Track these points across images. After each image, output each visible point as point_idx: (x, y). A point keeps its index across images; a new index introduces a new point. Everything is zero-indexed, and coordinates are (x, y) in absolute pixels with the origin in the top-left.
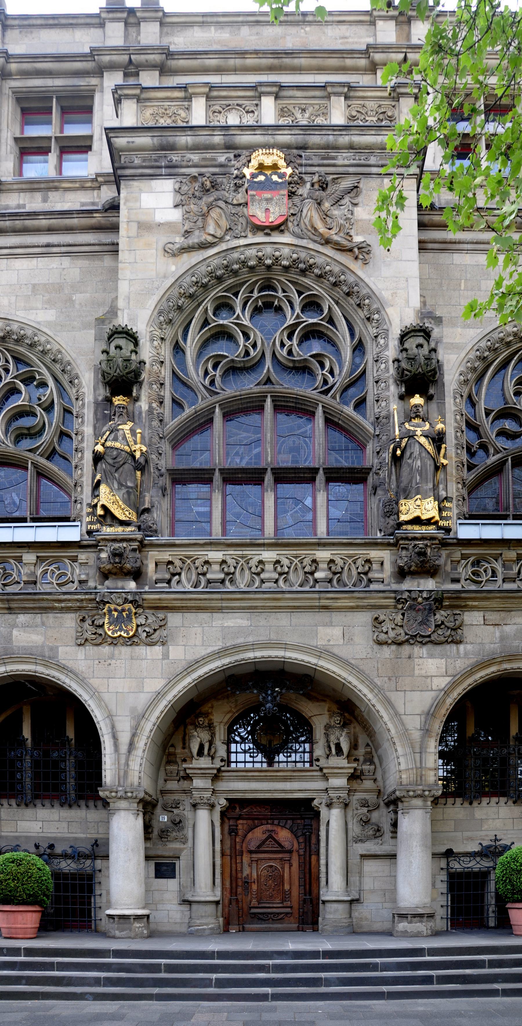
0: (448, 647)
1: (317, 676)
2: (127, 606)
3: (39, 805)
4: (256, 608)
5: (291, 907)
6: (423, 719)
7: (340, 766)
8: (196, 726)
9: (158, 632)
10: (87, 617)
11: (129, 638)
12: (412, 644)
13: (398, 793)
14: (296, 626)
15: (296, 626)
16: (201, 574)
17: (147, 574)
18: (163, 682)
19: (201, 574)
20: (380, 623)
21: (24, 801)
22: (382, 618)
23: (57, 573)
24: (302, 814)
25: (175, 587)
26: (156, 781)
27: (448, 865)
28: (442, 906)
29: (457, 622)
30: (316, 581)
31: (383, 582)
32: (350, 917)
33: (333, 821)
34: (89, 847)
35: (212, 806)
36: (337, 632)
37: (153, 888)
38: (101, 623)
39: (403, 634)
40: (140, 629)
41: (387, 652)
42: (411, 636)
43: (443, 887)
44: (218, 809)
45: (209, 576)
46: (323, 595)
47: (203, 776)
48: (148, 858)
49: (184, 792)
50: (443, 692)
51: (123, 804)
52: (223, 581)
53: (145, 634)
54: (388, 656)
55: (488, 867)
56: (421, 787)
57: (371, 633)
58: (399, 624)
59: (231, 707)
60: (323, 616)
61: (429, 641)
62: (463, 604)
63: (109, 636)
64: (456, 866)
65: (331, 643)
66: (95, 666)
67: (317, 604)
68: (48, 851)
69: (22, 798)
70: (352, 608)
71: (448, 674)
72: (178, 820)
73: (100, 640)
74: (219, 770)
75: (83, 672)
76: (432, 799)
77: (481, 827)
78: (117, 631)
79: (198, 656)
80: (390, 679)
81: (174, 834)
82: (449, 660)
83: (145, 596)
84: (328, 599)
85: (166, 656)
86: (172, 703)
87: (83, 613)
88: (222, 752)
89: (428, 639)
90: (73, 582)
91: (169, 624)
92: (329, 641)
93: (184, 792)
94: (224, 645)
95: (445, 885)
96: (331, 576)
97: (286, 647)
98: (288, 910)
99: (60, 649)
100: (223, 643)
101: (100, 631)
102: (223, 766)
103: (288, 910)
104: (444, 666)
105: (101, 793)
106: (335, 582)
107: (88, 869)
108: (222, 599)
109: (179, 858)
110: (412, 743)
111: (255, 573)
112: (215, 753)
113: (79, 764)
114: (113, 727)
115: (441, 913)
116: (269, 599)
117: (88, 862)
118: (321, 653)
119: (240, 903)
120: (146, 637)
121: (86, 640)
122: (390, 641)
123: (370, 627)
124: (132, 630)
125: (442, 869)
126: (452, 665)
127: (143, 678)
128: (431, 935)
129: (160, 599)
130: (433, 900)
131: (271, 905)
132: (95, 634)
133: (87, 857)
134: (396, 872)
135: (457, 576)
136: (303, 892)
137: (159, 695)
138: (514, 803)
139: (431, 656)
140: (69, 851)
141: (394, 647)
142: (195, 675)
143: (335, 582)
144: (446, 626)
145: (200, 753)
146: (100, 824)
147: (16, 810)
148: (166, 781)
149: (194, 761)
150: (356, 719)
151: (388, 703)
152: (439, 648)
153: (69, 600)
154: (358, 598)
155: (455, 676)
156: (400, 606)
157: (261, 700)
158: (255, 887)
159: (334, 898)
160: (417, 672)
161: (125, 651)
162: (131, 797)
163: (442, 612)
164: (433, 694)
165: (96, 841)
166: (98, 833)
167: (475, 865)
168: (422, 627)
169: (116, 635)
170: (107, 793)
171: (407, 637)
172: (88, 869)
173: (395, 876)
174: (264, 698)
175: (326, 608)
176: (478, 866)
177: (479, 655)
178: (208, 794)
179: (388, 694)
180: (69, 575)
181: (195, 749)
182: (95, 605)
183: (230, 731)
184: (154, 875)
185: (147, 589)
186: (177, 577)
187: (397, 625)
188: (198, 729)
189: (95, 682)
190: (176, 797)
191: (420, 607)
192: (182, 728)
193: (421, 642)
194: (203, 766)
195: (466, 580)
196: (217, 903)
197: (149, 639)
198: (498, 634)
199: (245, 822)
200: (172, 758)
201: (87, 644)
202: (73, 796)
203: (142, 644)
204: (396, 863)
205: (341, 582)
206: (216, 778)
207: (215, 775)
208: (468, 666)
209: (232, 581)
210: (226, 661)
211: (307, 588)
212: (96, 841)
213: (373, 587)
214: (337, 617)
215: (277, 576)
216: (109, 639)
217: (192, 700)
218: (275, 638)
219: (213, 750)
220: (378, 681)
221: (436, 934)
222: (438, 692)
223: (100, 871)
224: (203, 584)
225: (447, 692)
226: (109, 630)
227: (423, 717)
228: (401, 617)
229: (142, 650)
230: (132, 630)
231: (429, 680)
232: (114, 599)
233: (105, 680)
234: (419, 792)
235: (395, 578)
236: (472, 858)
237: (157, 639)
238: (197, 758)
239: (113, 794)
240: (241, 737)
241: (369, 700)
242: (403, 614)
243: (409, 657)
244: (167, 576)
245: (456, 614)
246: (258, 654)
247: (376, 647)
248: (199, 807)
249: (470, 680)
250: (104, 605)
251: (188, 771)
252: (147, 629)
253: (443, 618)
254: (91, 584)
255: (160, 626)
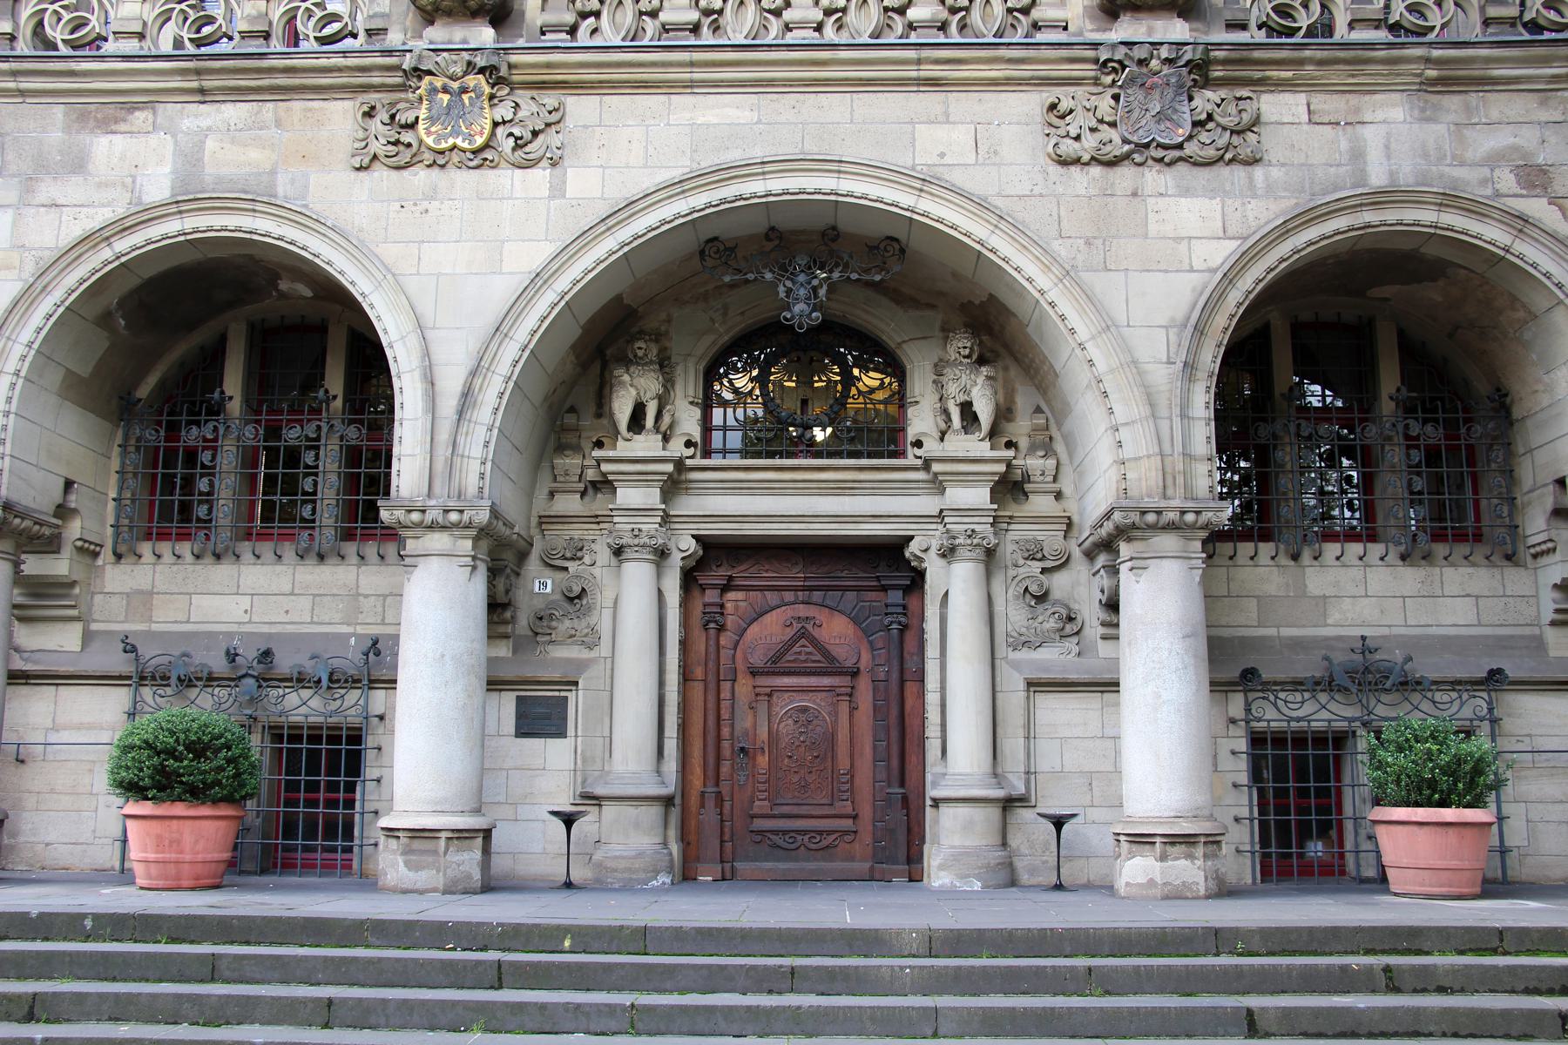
0: (1224, 171)
1: (916, 243)
2: (472, 80)
3: (247, 556)
4: (770, 82)
5: (855, 817)
6: (1173, 338)
7: (971, 454)
8: (627, 362)
9: (541, 137)
10: (379, 106)
11: (474, 152)
12: (1140, 165)
13: (1117, 516)
14: (864, 122)
15: (864, 122)
16: (646, 13)
17: (522, 13)
18: (549, 249)
19: (646, 13)
20: (1062, 117)
21: (210, 545)
22: (1064, 105)
23: (319, 14)
24: (881, 570)
25: (583, 38)
26: (530, 495)
27: (1248, 710)
28: (1237, 820)
29: (1244, 115)
30: (911, 26)
31: (1065, 28)
32: (1004, 844)
33: (954, 588)
34: (359, 658)
35: (662, 554)
36: (960, 137)
37: (509, 764)
38: (411, 119)
39: (1117, 140)
40: (500, 131)
41: (1084, 180)
42: (1137, 145)
43: (1240, 770)
44: (676, 560)
45: (663, 17)
46: (926, 53)
47: (642, 479)
48: (494, 684)
49: (596, 519)
50: (1219, 275)
51: (438, 541)
52: (695, 29)
53: (512, 140)
54: (1083, 192)
55: (1351, 720)
56: (1176, 503)
57: (1041, 139)
58: (1107, 119)
59: (712, 320)
60: (929, 101)
61: (1181, 159)
62: (1258, 75)
63: (430, 149)
64: (1272, 716)
65: (947, 160)
66: (392, 215)
67: (914, 74)
68: (258, 669)
69: (208, 537)
70: (994, 82)
71: (1230, 233)
72: (577, 590)
73: (406, 156)
74: (679, 464)
75: (361, 230)
76: (1204, 534)
77: (1325, 615)
78: (446, 138)
79: (634, 191)
80: (1088, 243)
81: (567, 623)
82: (1229, 202)
83: (514, 59)
84: (937, 62)
85: (558, 190)
86: (567, 298)
87: (373, 97)
88: (689, 423)
89: (1176, 153)
90: (355, 36)
91: (569, 122)
92: (942, 155)
93: (596, 519)
94: (695, 166)
95: (1243, 764)
96: (944, 14)
97: (837, 166)
98: (847, 824)
99: (312, 177)
100: (692, 160)
101: (407, 137)
102: (691, 457)
103: (847, 824)
104: (1218, 216)
105: (384, 515)
106: (953, 28)
107: (352, 712)
108: (692, 64)
109: (576, 684)
110: (1149, 395)
111: (769, 11)
112: (671, 427)
113: (352, 456)
114: (427, 353)
115: (1242, 837)
116: (801, 63)
117: (353, 695)
118: (925, 183)
119: (727, 805)
120: (514, 149)
121: (375, 157)
122: (1086, 157)
123: (1038, 128)
124: (481, 134)
125: (1233, 721)
126: (1238, 214)
127: (503, 242)
128: (1208, 897)
129: (549, 65)
130: (1216, 802)
131: (804, 810)
132: (397, 143)
133: (354, 682)
134: (1118, 725)
135: (1241, 16)
136: (884, 776)
137: (539, 280)
138: (1403, 558)
139: (1186, 192)
140: (309, 667)
141: (1096, 171)
142: (625, 234)
143: (953, 28)
144: (1218, 125)
145: (636, 421)
146: (389, 600)
147: (191, 568)
148: (552, 494)
149: (620, 443)
150: (1007, 346)
151: (1090, 298)
152: (1204, 173)
153: (339, 69)
154: (1010, 61)
155: (1245, 239)
156: (1108, 79)
157: (782, 295)
158: (763, 761)
159: (962, 793)
160: (1153, 228)
161: (462, 181)
162: (456, 525)
163: (1208, 94)
164: (1195, 279)
165: (375, 642)
166: (383, 623)
167: (1320, 713)
168: (1162, 127)
169: (444, 145)
170: (400, 514)
171: (1126, 148)
172: (352, 712)
173: (1116, 738)
174: (789, 291)
175: (934, 82)
176: (1325, 715)
177: (1303, 191)
178: (650, 525)
179: (1085, 276)
180: (346, 19)
181: (622, 411)
182: (398, 80)
183: (710, 376)
184: (513, 730)
185: (521, 43)
186: (592, 20)
187: (1101, 121)
188: (632, 369)
189: (389, 252)
190: (576, 532)
191: (1155, 79)
192: (596, 368)
193: (1160, 160)
194: (641, 454)
195: (1260, 27)
196: (668, 801)
197: (519, 153)
198: (1344, 145)
199: (740, 595)
200: (570, 438)
201: (377, 165)
202: (329, 533)
203: (503, 164)
204: (1118, 704)
205: (968, 31)
206: (674, 485)
207: (670, 475)
208: (1277, 217)
209: (716, 28)
210: (699, 200)
211: (891, 39)
212: (375, 642)
213: (1040, 37)
214: (961, 103)
215: (820, 16)
216: (428, 157)
217: (618, 298)
218: (816, 150)
219: (666, 419)
220: (1060, 248)
221: (1224, 891)
222: (1207, 274)
223: (381, 718)
224: (649, 33)
225: (1229, 277)
226: (429, 133)
227: (1172, 332)
228: (1112, 103)
229: (505, 179)
230: (481, 134)
231: (1183, 246)
232: (443, 64)
233: (414, 248)
234: (1172, 516)
235: (1092, 18)
236: (1307, 695)
237: (540, 153)
238: (628, 435)
239: (415, 517)
240: (736, 391)
241: (1042, 292)
242: (1116, 98)
243: (1135, 194)
244: (570, 18)
245: (1240, 99)
246: (776, 184)
247: (1055, 170)
248: (629, 554)
249: (1285, 248)
250: (420, 78)
251: (605, 467)
252: (517, 132)
253: (1209, 107)
254: (394, 39)
255: (548, 125)
